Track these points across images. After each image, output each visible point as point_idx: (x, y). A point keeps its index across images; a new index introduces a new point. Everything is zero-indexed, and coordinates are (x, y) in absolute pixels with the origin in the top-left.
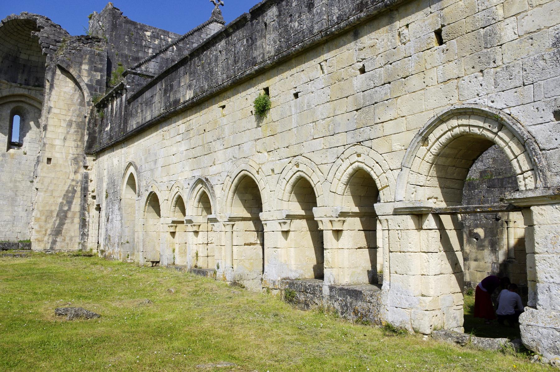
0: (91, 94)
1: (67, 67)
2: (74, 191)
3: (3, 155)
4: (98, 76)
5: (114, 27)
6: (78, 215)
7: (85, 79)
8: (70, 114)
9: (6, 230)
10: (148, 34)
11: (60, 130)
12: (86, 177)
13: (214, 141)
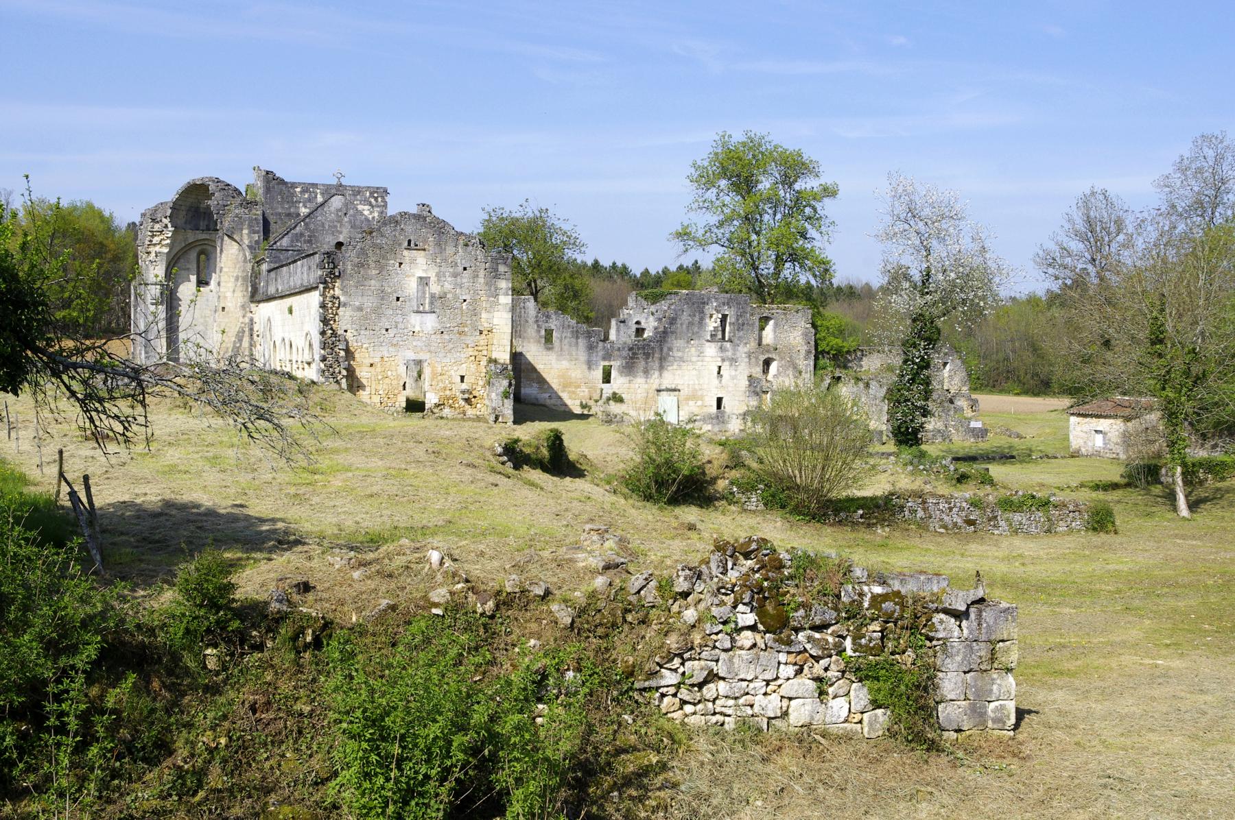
4: (256, 237)
5: (268, 190)
10: (298, 190)
11: (231, 285)
12: (252, 320)
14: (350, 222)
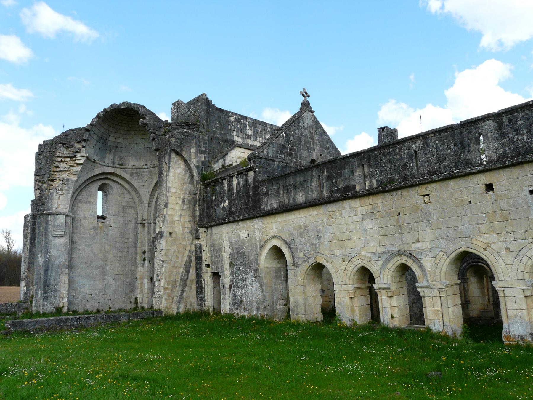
0: (199, 173)
1: (180, 151)
2: (191, 261)
3: (94, 228)
6: (194, 282)
7: (194, 162)
8: (183, 192)
9: (100, 298)
10: (232, 119)
11: (177, 207)
12: (200, 248)
13: (415, 222)
14: (319, 140)
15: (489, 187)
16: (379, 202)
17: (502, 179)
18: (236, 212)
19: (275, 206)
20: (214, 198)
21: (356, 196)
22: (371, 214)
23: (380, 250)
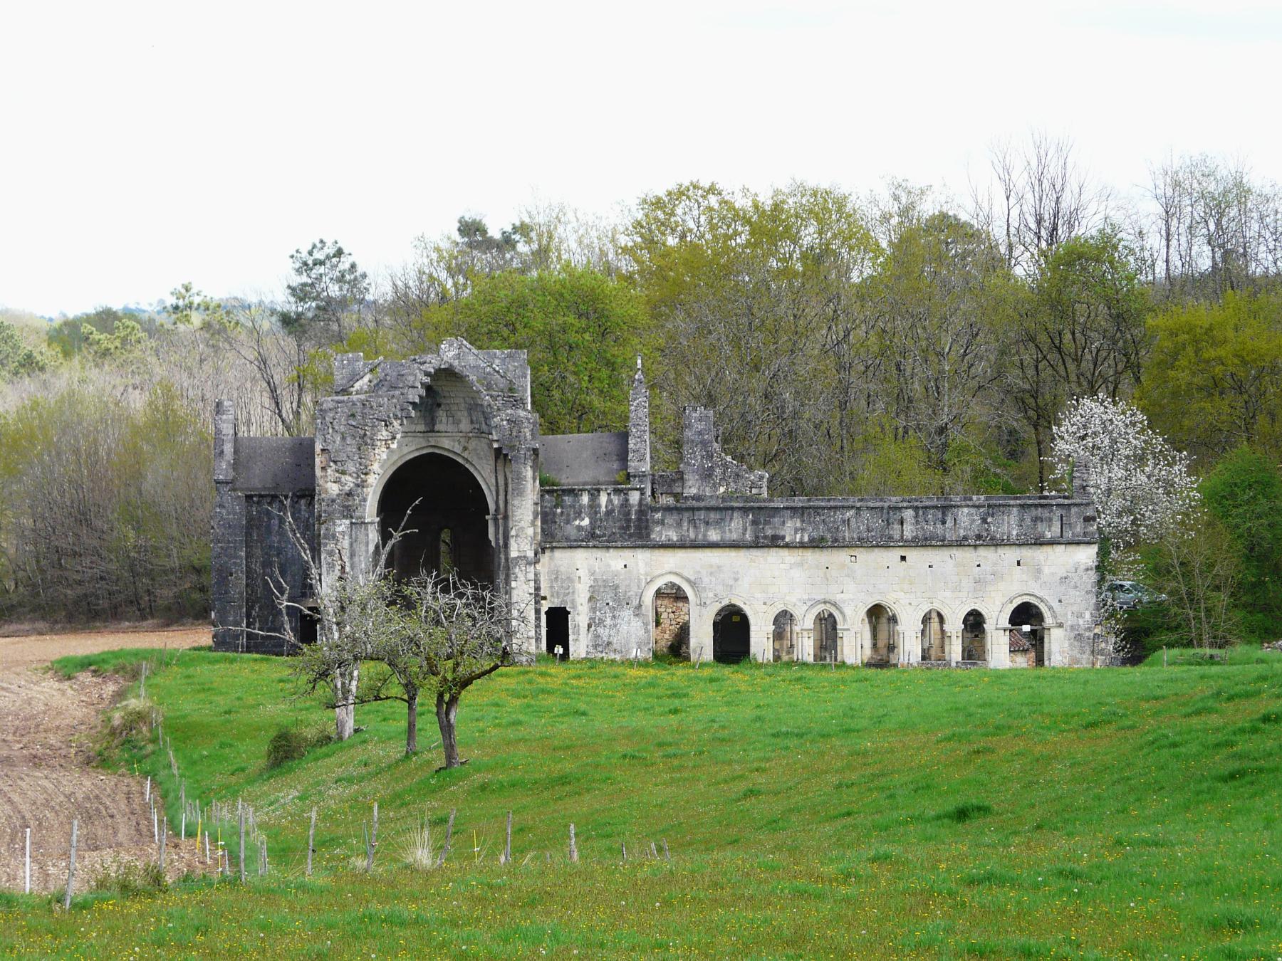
15: (903, 558)
16: (810, 556)
17: (912, 554)
18: (604, 535)
19: (675, 539)
20: (559, 510)
21: (787, 546)
22: (801, 565)
23: (806, 597)
